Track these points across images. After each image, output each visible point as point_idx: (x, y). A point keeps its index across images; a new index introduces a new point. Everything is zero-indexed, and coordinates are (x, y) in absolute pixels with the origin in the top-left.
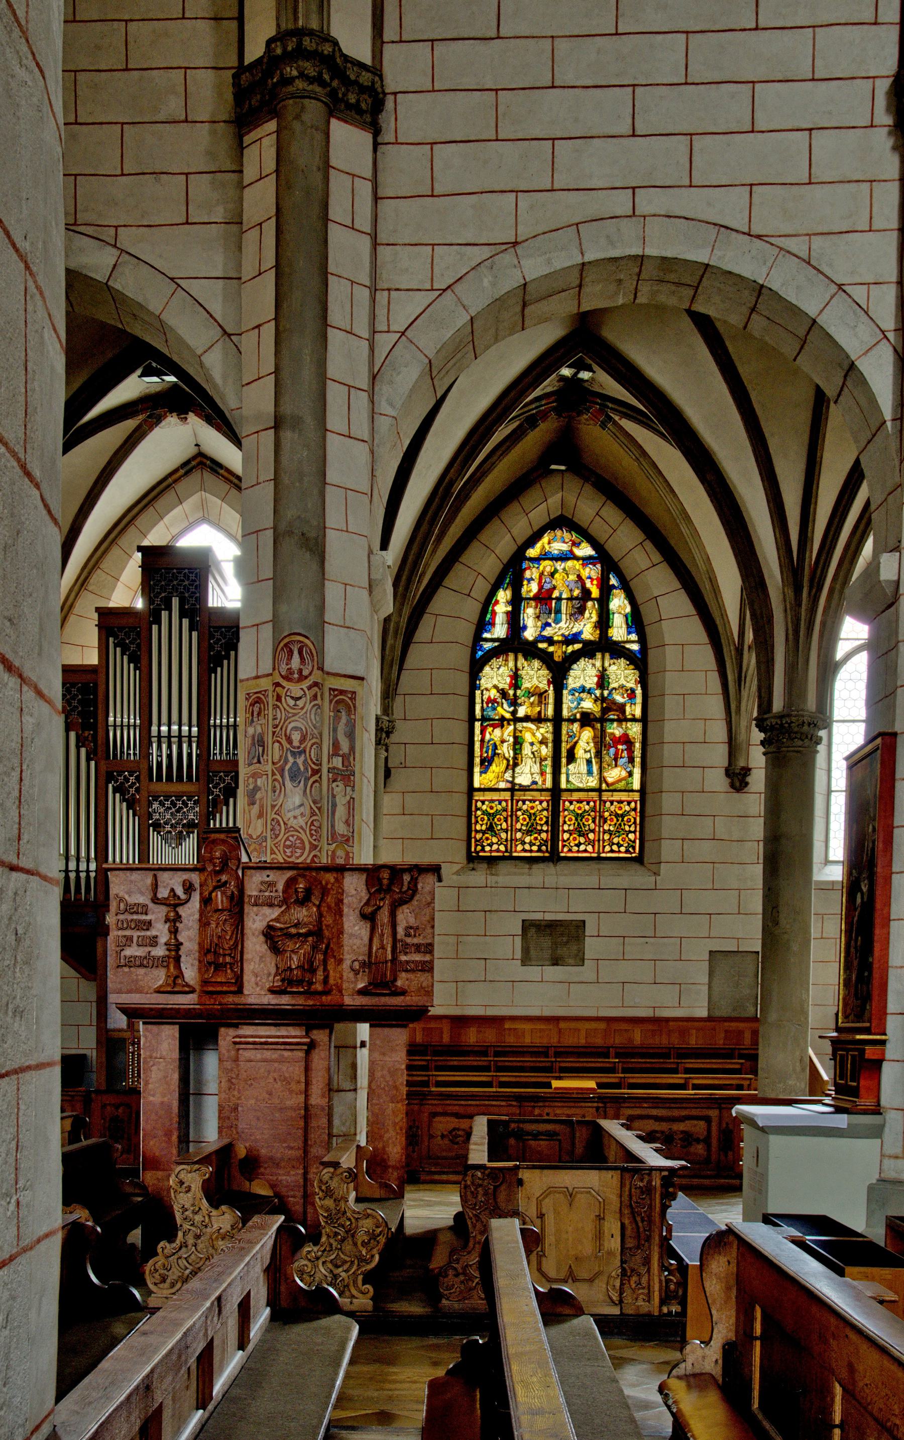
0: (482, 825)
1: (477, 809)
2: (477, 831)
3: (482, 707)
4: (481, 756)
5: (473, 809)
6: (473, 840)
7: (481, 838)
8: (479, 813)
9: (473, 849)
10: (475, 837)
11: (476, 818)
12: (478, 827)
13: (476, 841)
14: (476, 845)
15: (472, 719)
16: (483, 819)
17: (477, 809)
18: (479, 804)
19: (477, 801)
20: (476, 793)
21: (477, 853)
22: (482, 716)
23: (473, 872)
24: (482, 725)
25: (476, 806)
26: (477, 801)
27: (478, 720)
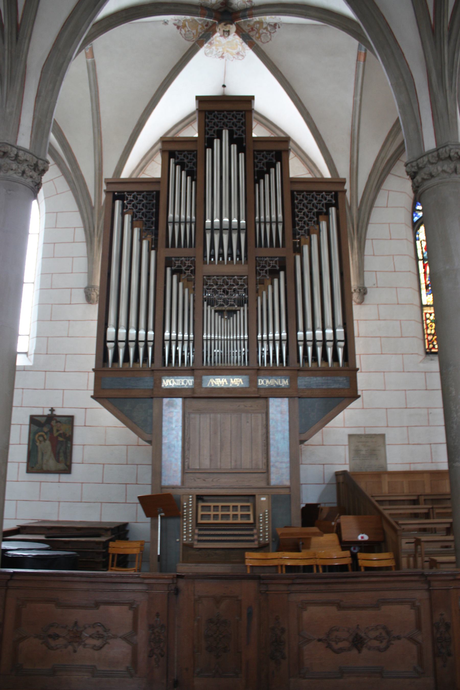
0: (431, 330)
1: (427, 319)
2: (429, 335)
3: (422, 252)
4: (426, 283)
5: (424, 318)
6: (426, 341)
7: (432, 339)
8: (428, 321)
9: (427, 347)
10: (427, 339)
11: (427, 325)
12: (429, 332)
13: (428, 341)
14: (429, 345)
15: (417, 259)
16: (431, 326)
17: (427, 319)
18: (428, 316)
19: (426, 314)
20: (425, 308)
21: (431, 349)
22: (423, 257)
23: (432, 362)
24: (423, 263)
25: (426, 317)
26: (426, 314)
27: (421, 260)
